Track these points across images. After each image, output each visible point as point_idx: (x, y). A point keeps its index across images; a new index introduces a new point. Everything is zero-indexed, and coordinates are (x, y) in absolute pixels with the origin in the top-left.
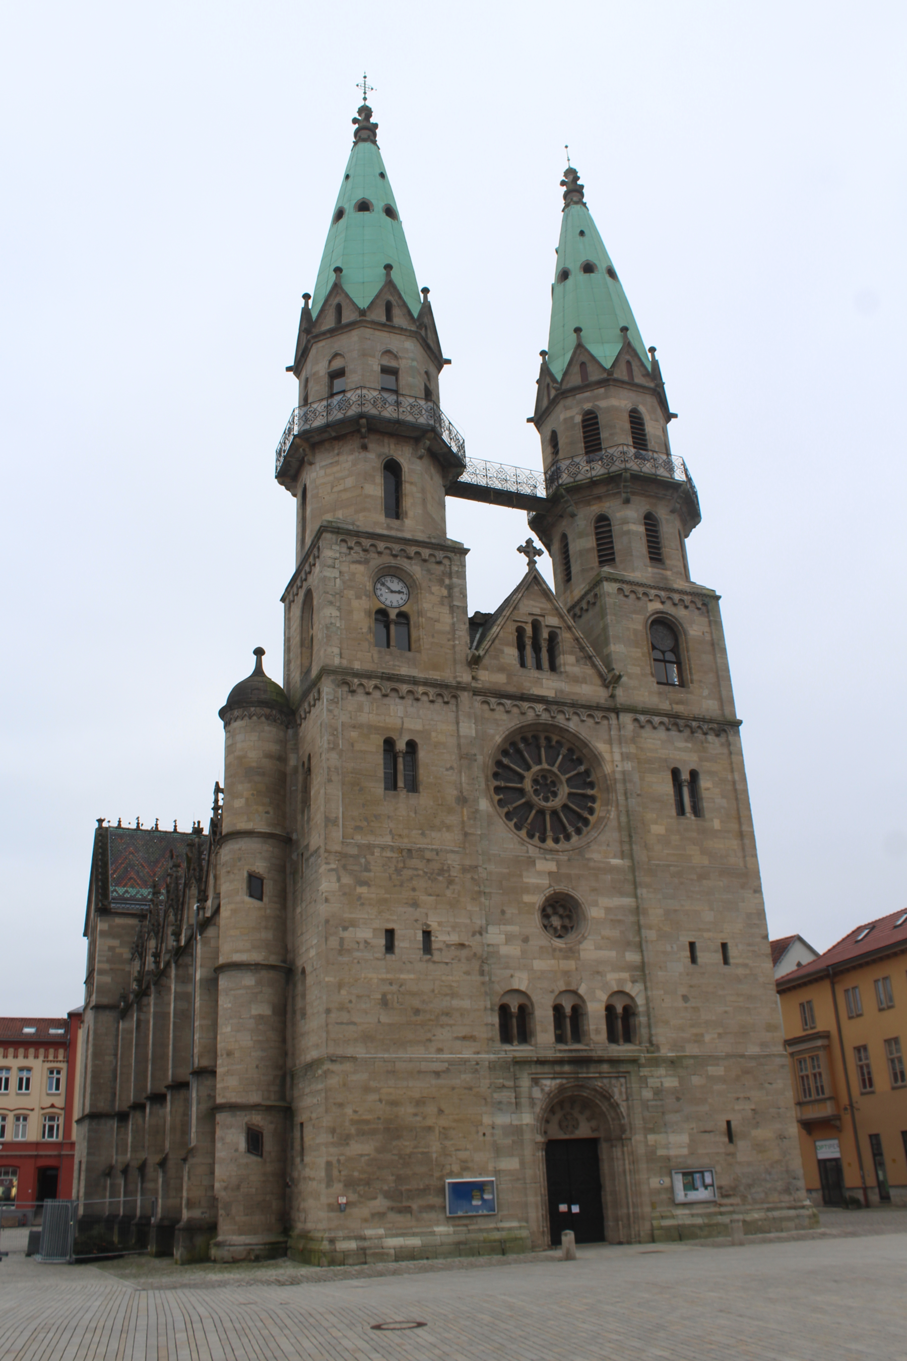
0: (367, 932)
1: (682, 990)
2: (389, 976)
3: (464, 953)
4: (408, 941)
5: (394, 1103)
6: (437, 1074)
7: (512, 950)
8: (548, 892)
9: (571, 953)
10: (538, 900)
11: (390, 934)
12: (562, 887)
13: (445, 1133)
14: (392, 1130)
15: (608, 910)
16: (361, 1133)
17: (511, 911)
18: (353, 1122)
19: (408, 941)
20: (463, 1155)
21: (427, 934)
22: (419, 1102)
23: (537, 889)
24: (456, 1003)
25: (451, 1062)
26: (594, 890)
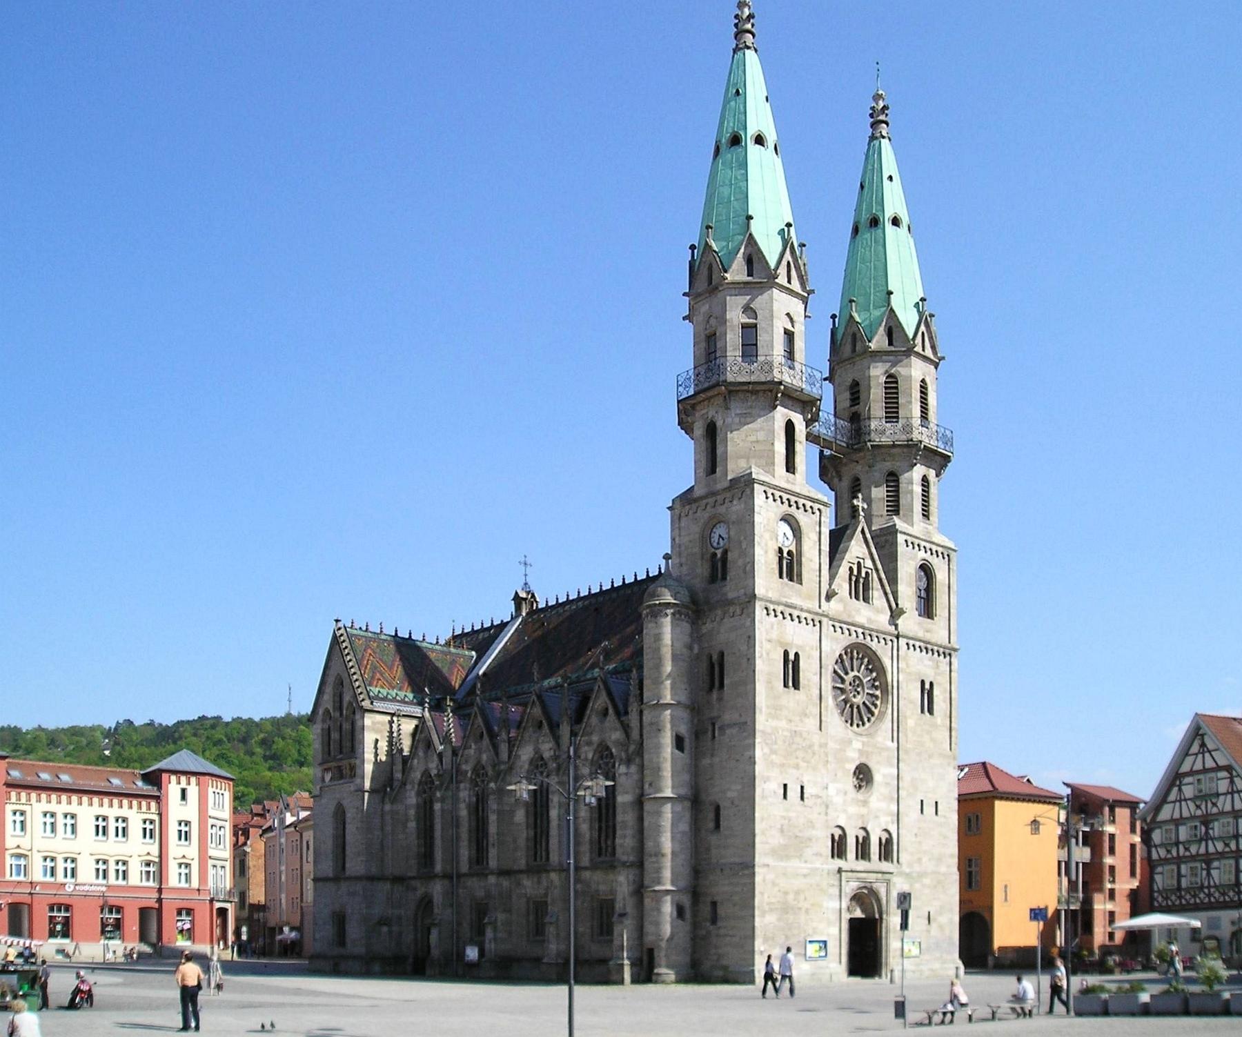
0: (775, 787)
1: (915, 831)
2: (784, 814)
3: (819, 801)
4: (794, 792)
5: (786, 893)
6: (805, 876)
7: (838, 800)
8: (857, 763)
9: (865, 803)
10: (853, 768)
11: (785, 786)
12: (863, 760)
13: (807, 911)
14: (785, 909)
15: (884, 776)
16: (771, 910)
17: (840, 774)
18: (769, 904)
19: (794, 792)
20: (815, 924)
21: (802, 787)
22: (797, 893)
23: (853, 760)
24: (814, 832)
25: (812, 869)
26: (878, 762)
